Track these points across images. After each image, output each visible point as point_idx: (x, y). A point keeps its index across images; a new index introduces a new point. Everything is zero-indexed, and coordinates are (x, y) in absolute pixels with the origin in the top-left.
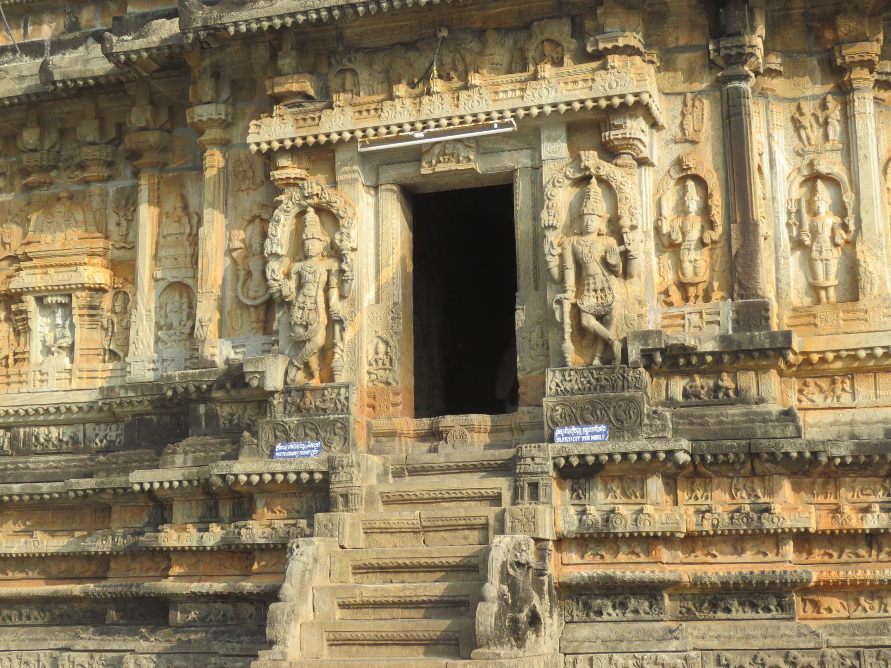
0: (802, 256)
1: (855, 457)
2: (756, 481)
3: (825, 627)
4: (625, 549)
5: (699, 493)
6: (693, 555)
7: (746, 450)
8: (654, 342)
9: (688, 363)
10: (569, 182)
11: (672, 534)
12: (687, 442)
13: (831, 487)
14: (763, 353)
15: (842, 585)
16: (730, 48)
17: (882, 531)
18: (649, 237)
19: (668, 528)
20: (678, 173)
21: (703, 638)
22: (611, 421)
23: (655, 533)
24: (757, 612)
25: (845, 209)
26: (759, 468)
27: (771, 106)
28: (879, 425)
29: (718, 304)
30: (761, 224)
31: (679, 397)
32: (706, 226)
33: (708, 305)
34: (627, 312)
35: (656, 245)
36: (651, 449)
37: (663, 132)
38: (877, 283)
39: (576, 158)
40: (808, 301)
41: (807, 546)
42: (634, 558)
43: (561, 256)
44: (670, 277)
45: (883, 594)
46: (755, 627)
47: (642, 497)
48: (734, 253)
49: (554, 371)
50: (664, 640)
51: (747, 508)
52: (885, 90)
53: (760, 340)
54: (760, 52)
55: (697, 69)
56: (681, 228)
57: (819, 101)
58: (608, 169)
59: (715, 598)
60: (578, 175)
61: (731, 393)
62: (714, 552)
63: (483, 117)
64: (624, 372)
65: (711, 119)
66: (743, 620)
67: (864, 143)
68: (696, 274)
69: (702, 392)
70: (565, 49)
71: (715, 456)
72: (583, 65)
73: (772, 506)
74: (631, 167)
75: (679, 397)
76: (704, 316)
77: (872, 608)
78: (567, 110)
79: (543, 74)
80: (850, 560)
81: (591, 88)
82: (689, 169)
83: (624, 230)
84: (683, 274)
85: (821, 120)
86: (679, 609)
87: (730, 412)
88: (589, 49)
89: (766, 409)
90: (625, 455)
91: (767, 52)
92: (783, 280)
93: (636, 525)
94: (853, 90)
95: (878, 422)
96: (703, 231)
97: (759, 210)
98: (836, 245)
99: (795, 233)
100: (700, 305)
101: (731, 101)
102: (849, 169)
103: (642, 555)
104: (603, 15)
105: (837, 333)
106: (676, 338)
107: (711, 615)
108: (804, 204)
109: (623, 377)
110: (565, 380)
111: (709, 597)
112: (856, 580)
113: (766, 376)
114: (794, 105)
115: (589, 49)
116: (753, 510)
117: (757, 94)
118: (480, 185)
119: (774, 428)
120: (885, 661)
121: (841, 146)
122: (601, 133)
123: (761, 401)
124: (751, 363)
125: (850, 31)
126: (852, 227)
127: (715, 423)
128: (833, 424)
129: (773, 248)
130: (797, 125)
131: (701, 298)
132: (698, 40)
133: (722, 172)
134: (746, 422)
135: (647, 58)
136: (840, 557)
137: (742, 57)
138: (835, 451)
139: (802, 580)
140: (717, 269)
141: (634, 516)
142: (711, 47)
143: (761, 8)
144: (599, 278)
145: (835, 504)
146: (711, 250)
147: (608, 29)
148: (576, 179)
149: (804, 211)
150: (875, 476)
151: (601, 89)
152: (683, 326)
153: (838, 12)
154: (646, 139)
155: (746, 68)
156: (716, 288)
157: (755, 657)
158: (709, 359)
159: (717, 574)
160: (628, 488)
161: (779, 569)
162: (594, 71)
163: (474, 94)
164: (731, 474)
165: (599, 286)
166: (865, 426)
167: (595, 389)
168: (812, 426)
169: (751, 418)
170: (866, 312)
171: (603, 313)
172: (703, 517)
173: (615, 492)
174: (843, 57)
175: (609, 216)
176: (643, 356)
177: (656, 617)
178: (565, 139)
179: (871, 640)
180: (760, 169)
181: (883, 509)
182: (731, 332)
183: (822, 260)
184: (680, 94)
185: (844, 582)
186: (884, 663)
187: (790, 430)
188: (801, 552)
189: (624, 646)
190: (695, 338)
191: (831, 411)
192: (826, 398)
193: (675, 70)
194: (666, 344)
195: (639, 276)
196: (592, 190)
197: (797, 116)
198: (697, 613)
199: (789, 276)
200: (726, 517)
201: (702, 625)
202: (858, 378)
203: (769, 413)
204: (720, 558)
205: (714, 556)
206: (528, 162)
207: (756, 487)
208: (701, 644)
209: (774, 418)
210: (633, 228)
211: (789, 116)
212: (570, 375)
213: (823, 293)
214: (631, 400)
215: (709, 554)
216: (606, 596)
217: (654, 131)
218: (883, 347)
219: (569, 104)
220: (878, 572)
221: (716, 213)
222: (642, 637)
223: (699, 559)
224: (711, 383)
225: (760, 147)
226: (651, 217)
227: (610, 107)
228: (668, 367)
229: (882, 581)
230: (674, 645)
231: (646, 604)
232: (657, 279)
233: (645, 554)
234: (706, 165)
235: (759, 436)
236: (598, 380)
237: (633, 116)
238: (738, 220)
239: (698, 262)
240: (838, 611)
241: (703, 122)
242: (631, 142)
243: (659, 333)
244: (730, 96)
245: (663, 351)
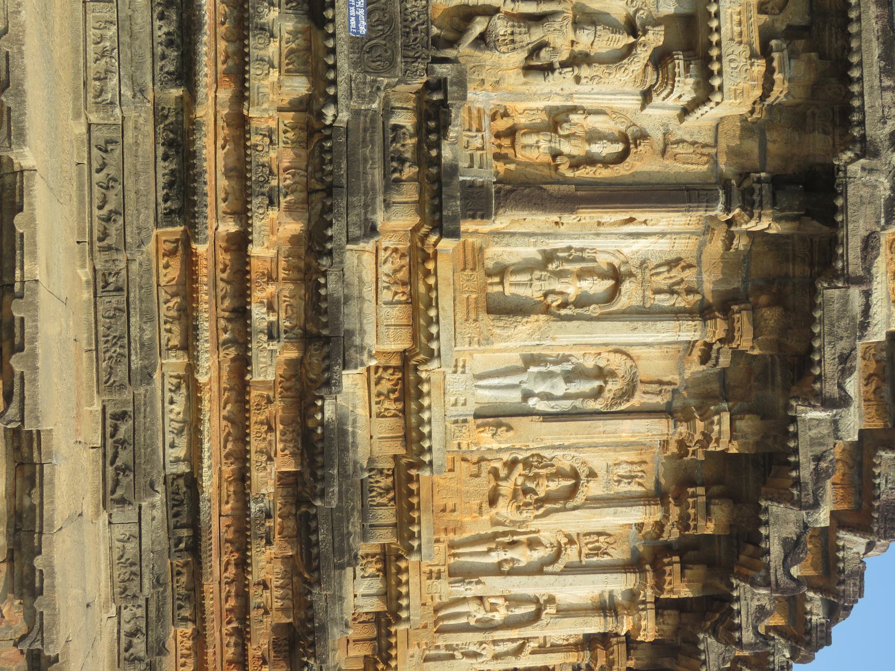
0: (537, 261)
1: (325, 298)
2: (303, 195)
3: (149, 260)
4: (232, 48)
5: (290, 135)
6: (225, 124)
7: (335, 183)
8: (454, 92)
9: (430, 131)
10: (631, 13)
11: (248, 98)
12: (346, 119)
13: (295, 275)
14: (438, 209)
15: (193, 279)
16: (760, 194)
17: (248, 322)
18: (567, 100)
19: (253, 94)
21: (135, 128)
22: (370, 40)
23: (248, 80)
24: (163, 188)
25: (582, 307)
26: (316, 197)
27: (695, 237)
28: (358, 326)
29: (491, 167)
30: (574, 216)
31: (394, 121)
32: (574, 160)
33: (490, 157)
34: (487, 67)
35: (557, 108)
36: (339, 79)
38: (505, 333)
39: (657, 23)
40: (490, 264)
41: (233, 248)
42: (221, 58)
44: (523, 120)
45: (183, 320)
46: (148, 184)
47: (288, 71)
48: (544, 186)
50: (133, 83)
51: (274, 183)
52: (700, 357)
53: (452, 206)
54: (753, 226)
56: (573, 135)
57: (696, 287)
58: (642, 56)
59: (179, 145)
60: (638, 22)
61: (396, 175)
62: (227, 147)
64: (423, 59)
66: (156, 173)
67: (649, 328)
68: (524, 147)
69: (399, 145)
70: (776, 17)
71: (330, 150)
72: (758, 38)
73: (276, 208)
74: (643, 82)
75: (394, 121)
76: (479, 152)
77: (168, 309)
78: (710, 13)
80: (218, 290)
81: (732, 39)
82: (636, 147)
83: (576, 69)
84: (524, 134)
85: (676, 288)
86: (167, 107)
87: (376, 172)
88: (773, 43)
89: (378, 210)
90: (333, 51)
91: (751, 234)
92: (513, 240)
93: (257, 60)
94: (705, 320)
95: (361, 324)
96: (570, 157)
97: (587, 216)
98: (546, 295)
99: (561, 255)
100: (491, 149)
101: (705, 192)
102: (624, 312)
103: (225, 66)
104: (810, 59)
105: (455, 290)
106: (457, 116)
107: (161, 141)
108: (591, 265)
109: (418, 57)
111: (179, 139)
112: (198, 292)
113: (413, 211)
114: (693, 261)
115: (773, 43)
116: (272, 189)
117: (709, 223)
119: (358, 215)
120: (114, 317)
121: (648, 305)
122: (683, 51)
123: (387, 205)
124: (427, 197)
125: (766, 320)
126: (563, 312)
127: (365, 155)
128: (361, 280)
129: (546, 231)
130: (672, 264)
131: (498, 151)
132: (773, 163)
133: (630, 180)
134: (365, 187)
135: (758, 107)
136: (222, 280)
137: (750, 206)
138: (332, 278)
139: (197, 233)
140: (528, 169)
141: (267, 59)
142: (763, 175)
143: (799, 229)
144: (526, 39)
145: (277, 278)
146: (549, 164)
147: (793, 62)
148: (635, 21)
149: (584, 265)
150: (306, 320)
151: (730, 51)
152: (469, 130)
153: (786, 309)
154: (670, 101)
155: (737, 211)
156: (508, 166)
157: (115, 180)
158: (434, 153)
159: (204, 147)
160: (298, 57)
161: (209, 211)
162: (751, 45)
164: (310, 169)
165: (517, 38)
166: (357, 311)
167: (405, 27)
168: (359, 258)
169: (369, 192)
170: (476, 320)
171: (488, 40)
172: (265, 136)
173: (294, 42)
174: (739, 312)
175: (592, 54)
176: (439, 81)
177: (157, 78)
178: (678, 12)
179: (135, 304)
180: (631, 220)
181: (271, 324)
182: (461, 178)
183: (531, 280)
184: (716, 141)
185: (196, 281)
186: (111, 315)
187: (356, 232)
188: (227, 241)
189: (125, 39)
190: (456, 138)
191: (374, 280)
192: (388, 275)
193: (741, 138)
194: (452, 105)
195: (525, 84)
196: (621, 37)
197: (683, 264)
198: (162, 126)
199: (517, 246)
200: (265, 159)
201: (149, 128)
202: (408, 309)
203: (374, 212)
204: (221, 153)
205: (223, 147)
207: (297, 194)
208: (130, 125)
209: (369, 216)
210: (578, 79)
211: (683, 256)
213: (497, 279)
214: (392, 63)
215: (226, 141)
216: (180, 26)
217: (678, 112)
218: (438, 333)
219: (717, 15)
220: (206, 315)
221: (587, 171)
222: (136, 59)
223: (219, 130)
224: (408, 155)
225: (653, 222)
226: (587, 103)
227: (710, 60)
228: (426, 110)
229: (197, 319)
230: (127, 93)
231: (172, 69)
232: (520, 106)
233: (226, 69)
234: (638, 163)
235: (350, 199)
236: (416, 30)
237: (697, 86)
238: (579, 193)
240: (165, 275)
241: (684, 163)
242: (670, 82)
243: (464, 98)
244: (709, 192)
245: (443, 103)
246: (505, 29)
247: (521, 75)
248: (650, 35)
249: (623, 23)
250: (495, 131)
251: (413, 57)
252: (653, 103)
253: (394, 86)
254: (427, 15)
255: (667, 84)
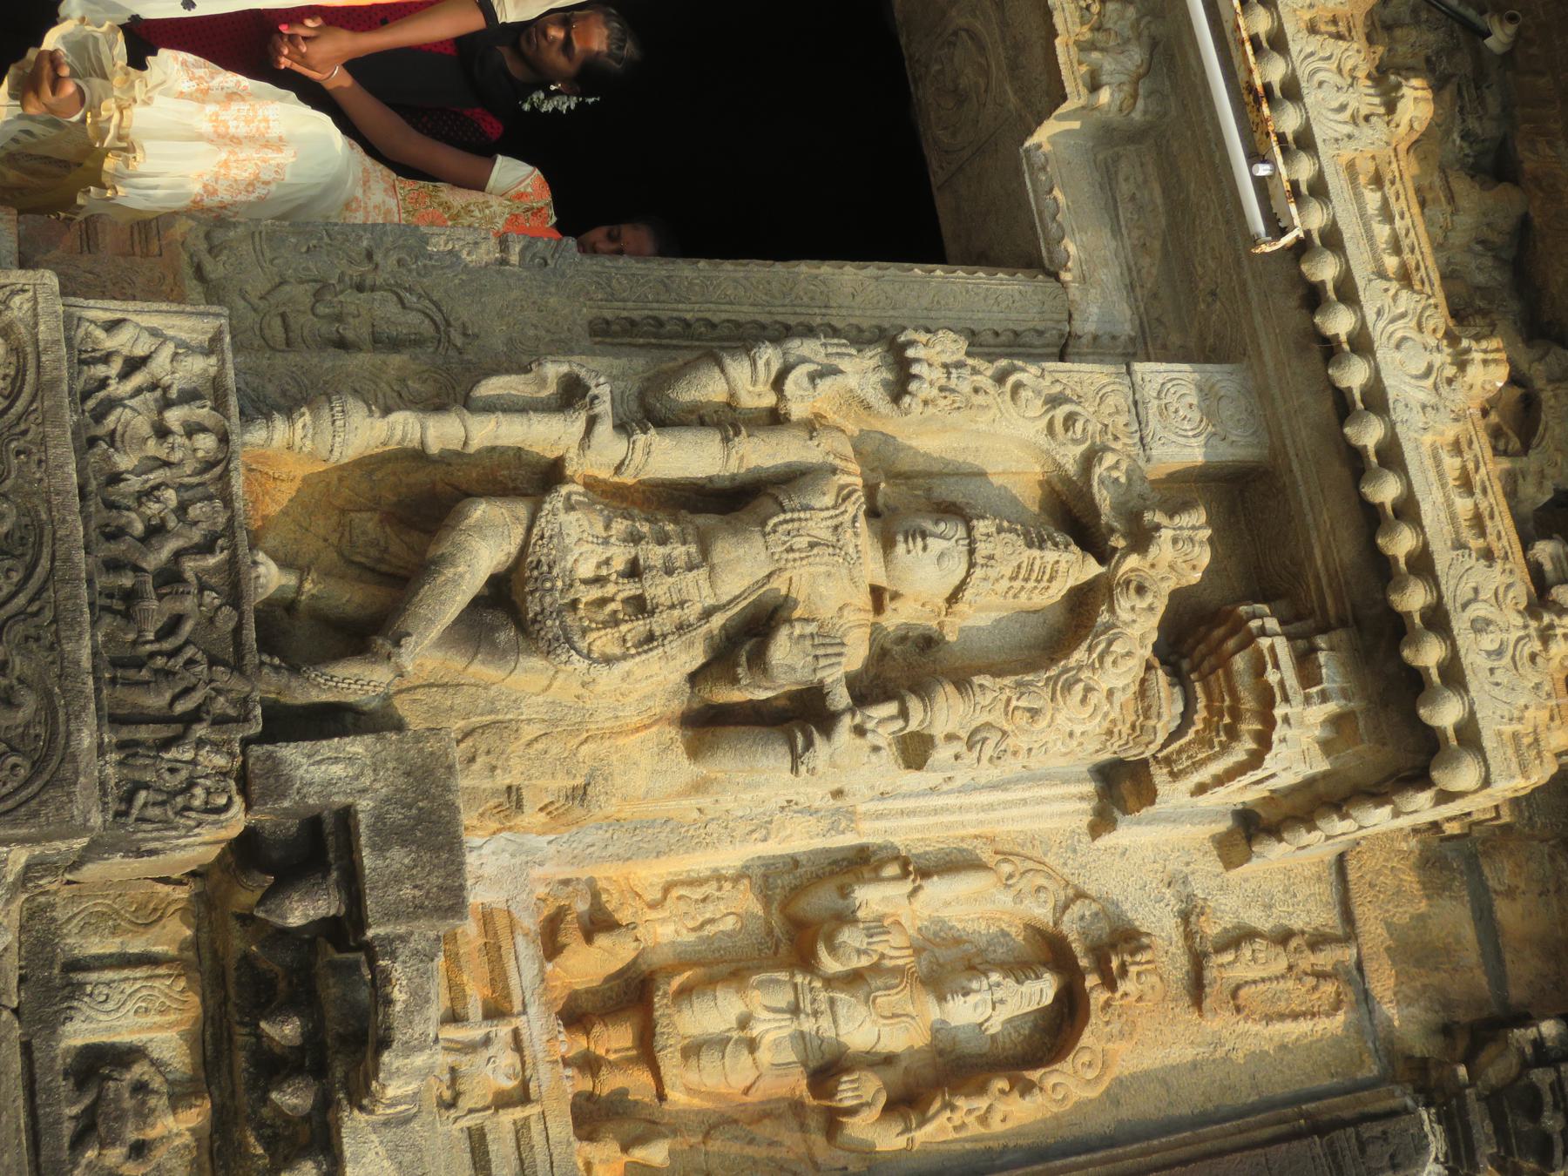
8: (397, 879)
10: (1071, 468)
18: (834, 828)
20: (1084, 934)
33: (561, 1127)
34: (529, 732)
35: (794, 862)
37: (1213, 864)
43: (775, 419)
49: (212, 347)
55: (1436, 979)
58: (1135, 632)
60: (1104, 499)
63: (1289, 121)
64: (220, 721)
65: (1283, 1047)
68: (693, 1050)
69: (115, 1155)
75: (80, 1032)
76: (509, 1117)
79: (1477, 356)
82: (1110, 983)
83: (914, 704)
84: (685, 992)
101: (1377, 1128)
106: (420, 998)
109: (193, 717)
110: (167, 404)
118: (937, 177)
131: (586, 1084)
140: (715, 1145)
144: (697, 590)
146: (797, 1107)
151: (1465, 592)
152: (454, 1017)
163: (1365, 98)
165: (658, 589)
167: (114, 566)
171: (533, 608)
175: (951, 637)
176: (313, 824)
184: (1348, 916)
194: (389, 946)
196: (1065, 556)
206: (1089, 321)
212: (192, 430)
221: (958, 1118)
232: (650, 874)
234: (1121, 1048)
236: (170, 577)
239: (745, 1057)
241: (1268, 1019)
243: (451, 902)
244: (1392, 1126)
246: (601, 553)
247: (680, 748)
248: (1163, 549)
249: (1035, 509)
250: (560, 995)
251: (167, 720)
252: (1159, 807)
253: (75, 866)
254: (228, 502)
255: (1233, 734)
